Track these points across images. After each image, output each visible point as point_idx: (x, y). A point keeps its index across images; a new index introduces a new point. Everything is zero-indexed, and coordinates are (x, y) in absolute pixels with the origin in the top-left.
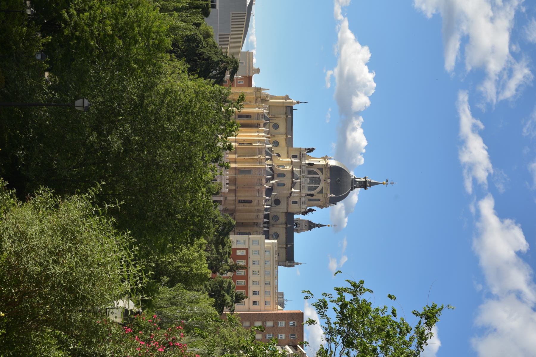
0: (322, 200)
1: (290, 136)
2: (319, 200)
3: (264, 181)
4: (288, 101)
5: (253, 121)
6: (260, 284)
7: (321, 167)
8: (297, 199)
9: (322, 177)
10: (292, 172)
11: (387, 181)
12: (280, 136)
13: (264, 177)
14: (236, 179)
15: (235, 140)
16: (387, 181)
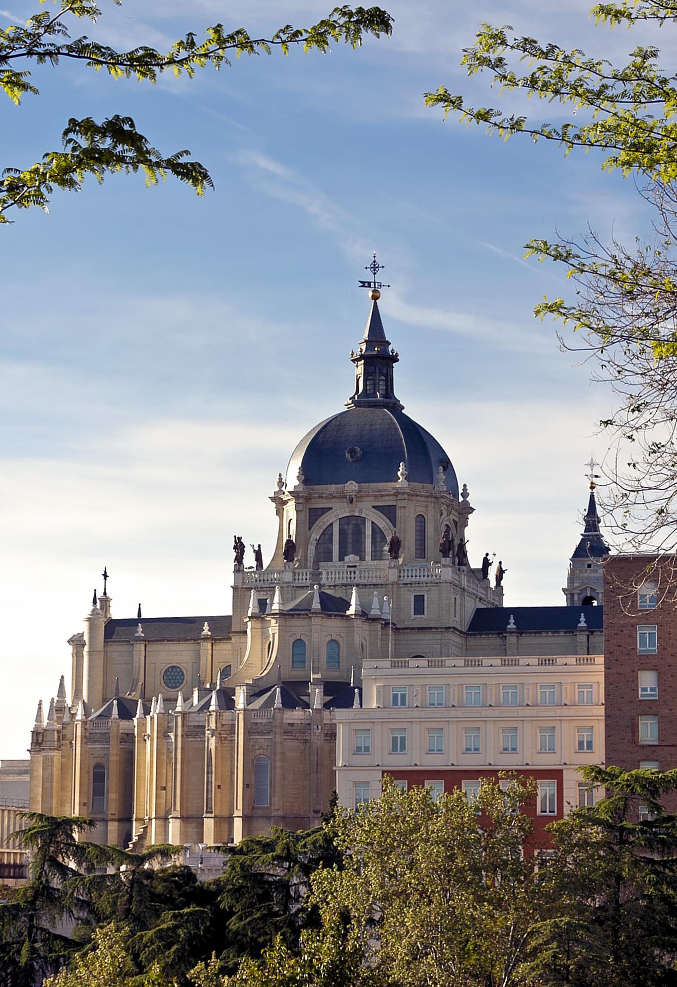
0: (421, 510)
1: (206, 627)
2: (421, 520)
3: (296, 715)
4: (86, 638)
5: (111, 758)
6: (404, 726)
7: (306, 515)
8: (409, 598)
9: (340, 510)
10: (282, 615)
11: (364, 284)
12: (205, 660)
13: (278, 715)
14: (284, 817)
15: (161, 822)
16: (364, 284)
